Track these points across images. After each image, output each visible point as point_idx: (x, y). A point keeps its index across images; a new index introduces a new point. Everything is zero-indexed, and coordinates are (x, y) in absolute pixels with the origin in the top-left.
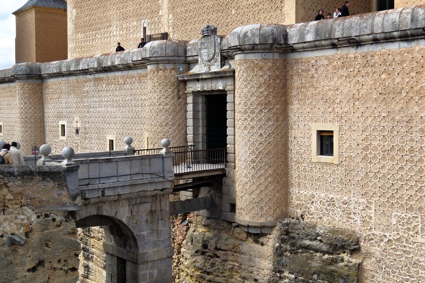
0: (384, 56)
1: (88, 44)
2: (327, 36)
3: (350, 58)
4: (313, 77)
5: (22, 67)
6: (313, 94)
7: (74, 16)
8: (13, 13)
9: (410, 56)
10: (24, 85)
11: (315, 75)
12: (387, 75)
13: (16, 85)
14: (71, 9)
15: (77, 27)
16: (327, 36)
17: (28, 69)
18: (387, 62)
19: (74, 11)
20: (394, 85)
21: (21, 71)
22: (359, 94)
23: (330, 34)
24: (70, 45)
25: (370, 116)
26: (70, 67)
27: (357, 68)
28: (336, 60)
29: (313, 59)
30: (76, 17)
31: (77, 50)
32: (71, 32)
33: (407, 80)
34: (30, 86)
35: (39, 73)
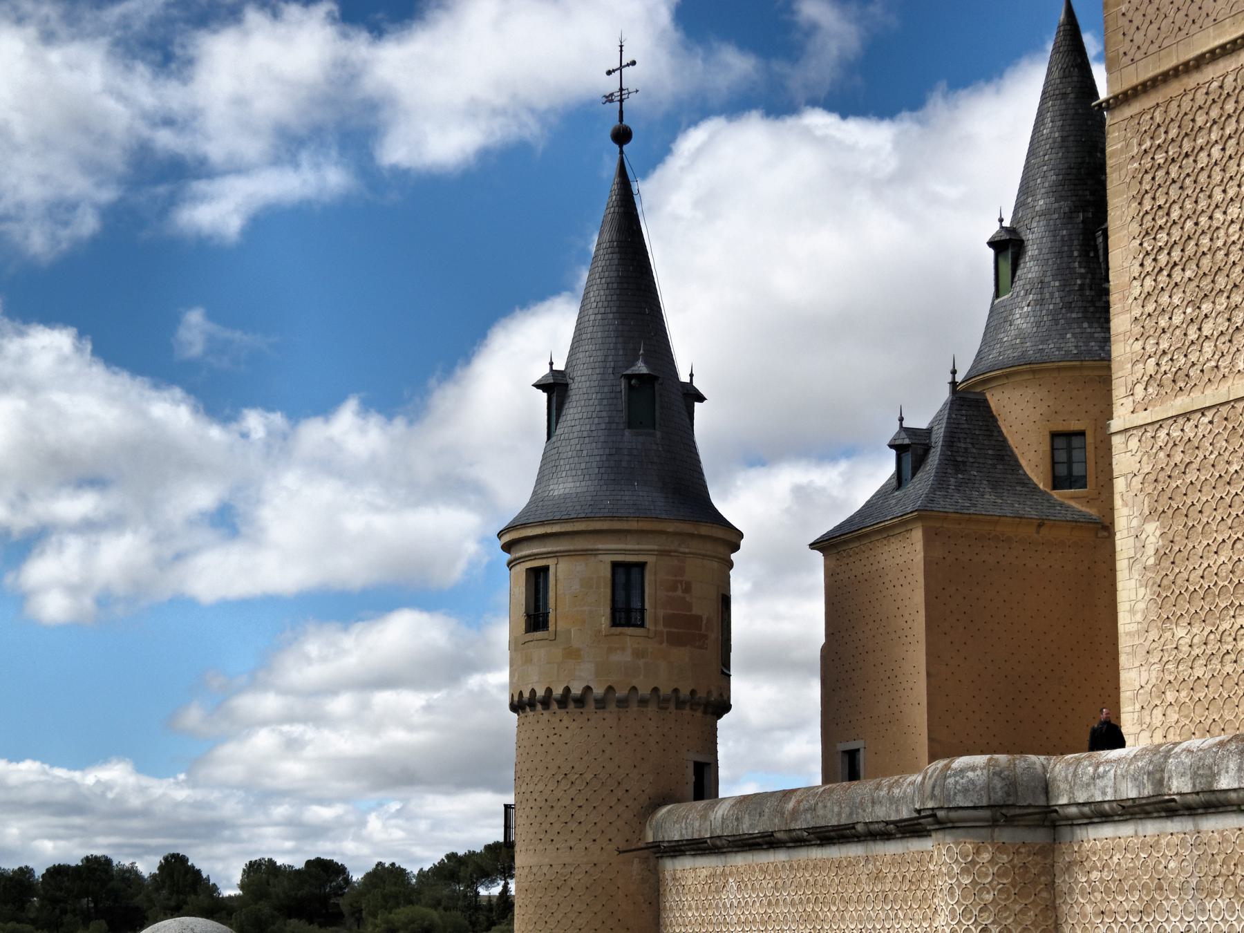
1: (1229, 668)
5: (970, 774)
7: (1150, 550)
8: (813, 546)
10: (977, 852)
13: (939, 854)
14: (1135, 523)
15: (1168, 597)
17: (998, 783)
19: (1153, 529)
21: (965, 791)
24: (1134, 676)
26: (1214, 776)
30: (1161, 555)
31: (1170, 696)
32: (1139, 617)
34: (1005, 858)
35: (1042, 802)
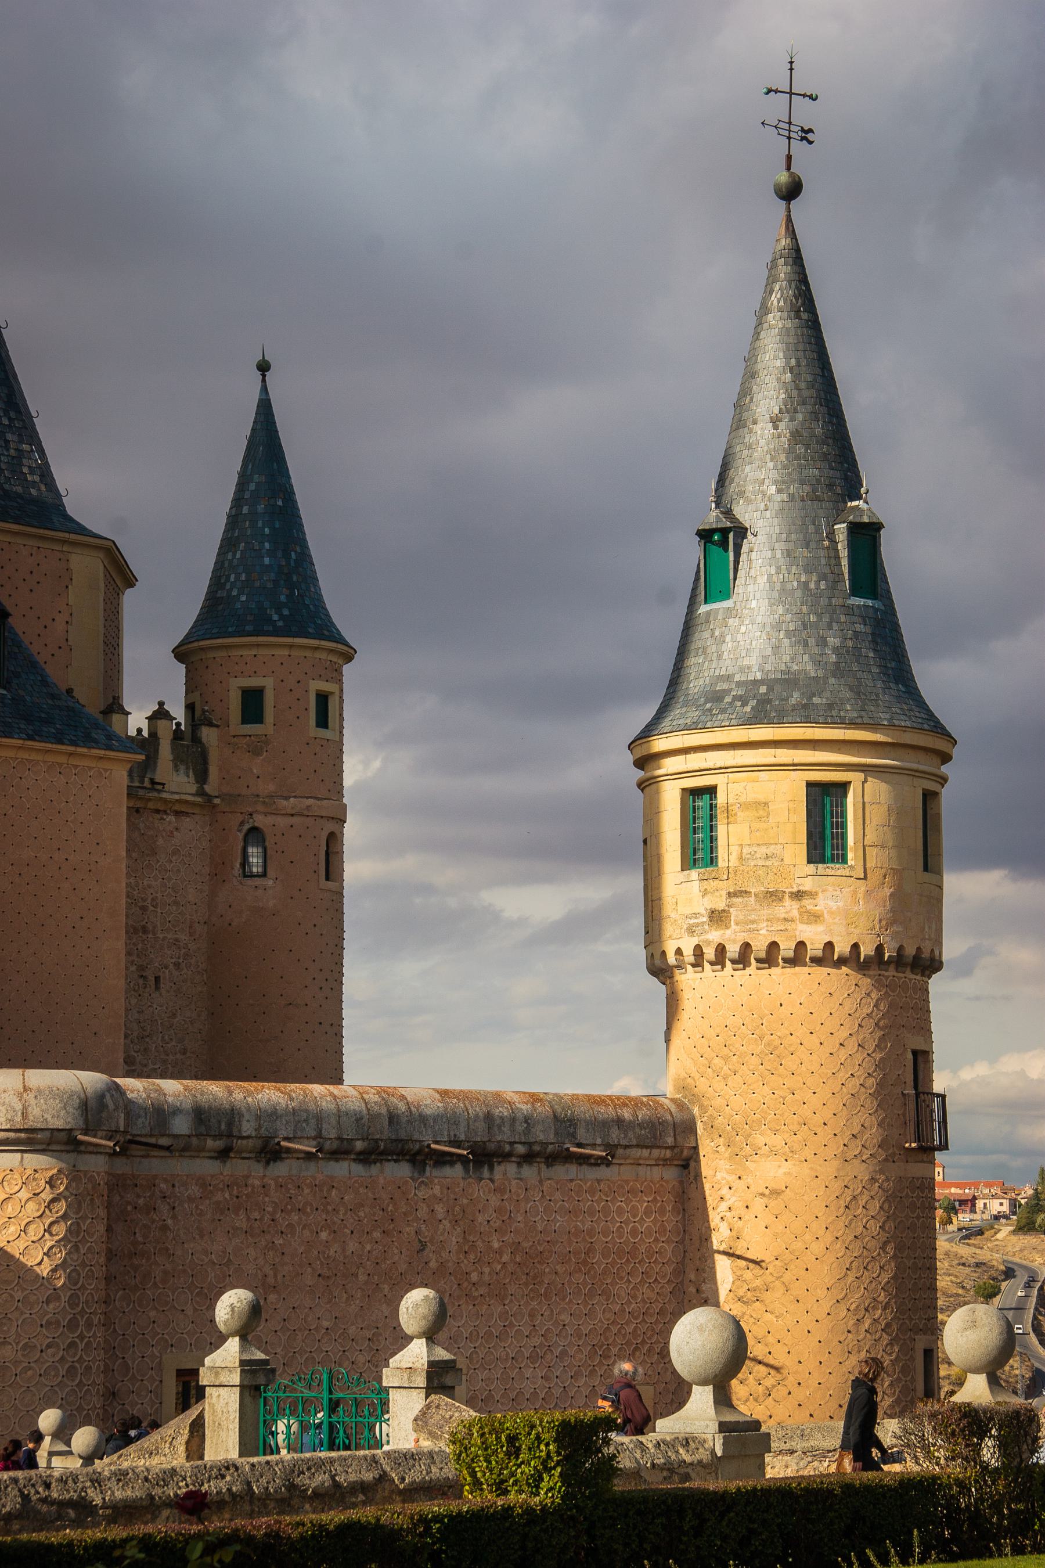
0: (321, 1191)
2: (223, 1127)
3: (253, 1186)
4: (165, 1228)
6: (165, 1272)
9: (370, 1194)
11: (169, 1222)
12: (329, 1234)
16: (223, 1127)
18: (328, 1204)
20: (345, 1257)
22: (275, 1276)
23: (230, 1125)
25: (300, 1329)
27: (268, 1212)
28: (222, 1190)
29: (165, 1181)
33: (368, 1247)
